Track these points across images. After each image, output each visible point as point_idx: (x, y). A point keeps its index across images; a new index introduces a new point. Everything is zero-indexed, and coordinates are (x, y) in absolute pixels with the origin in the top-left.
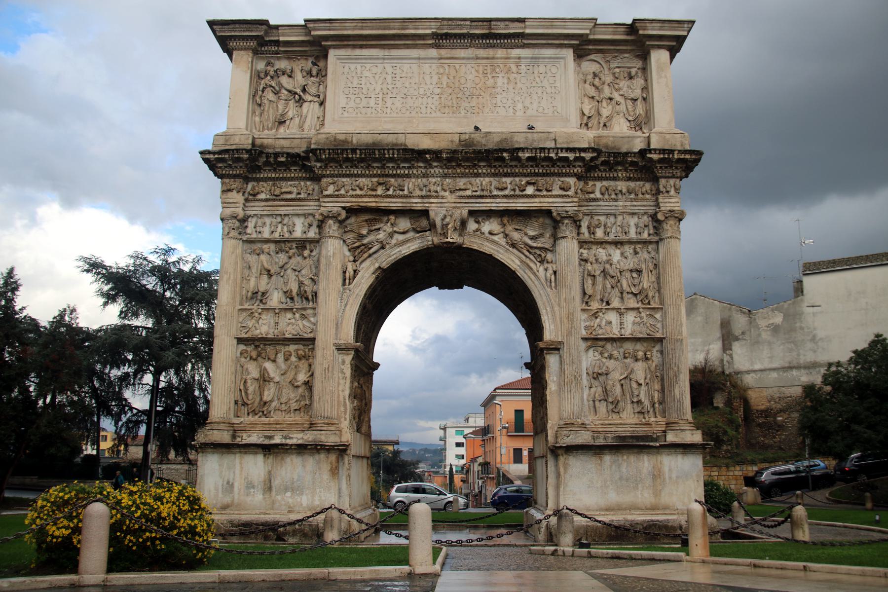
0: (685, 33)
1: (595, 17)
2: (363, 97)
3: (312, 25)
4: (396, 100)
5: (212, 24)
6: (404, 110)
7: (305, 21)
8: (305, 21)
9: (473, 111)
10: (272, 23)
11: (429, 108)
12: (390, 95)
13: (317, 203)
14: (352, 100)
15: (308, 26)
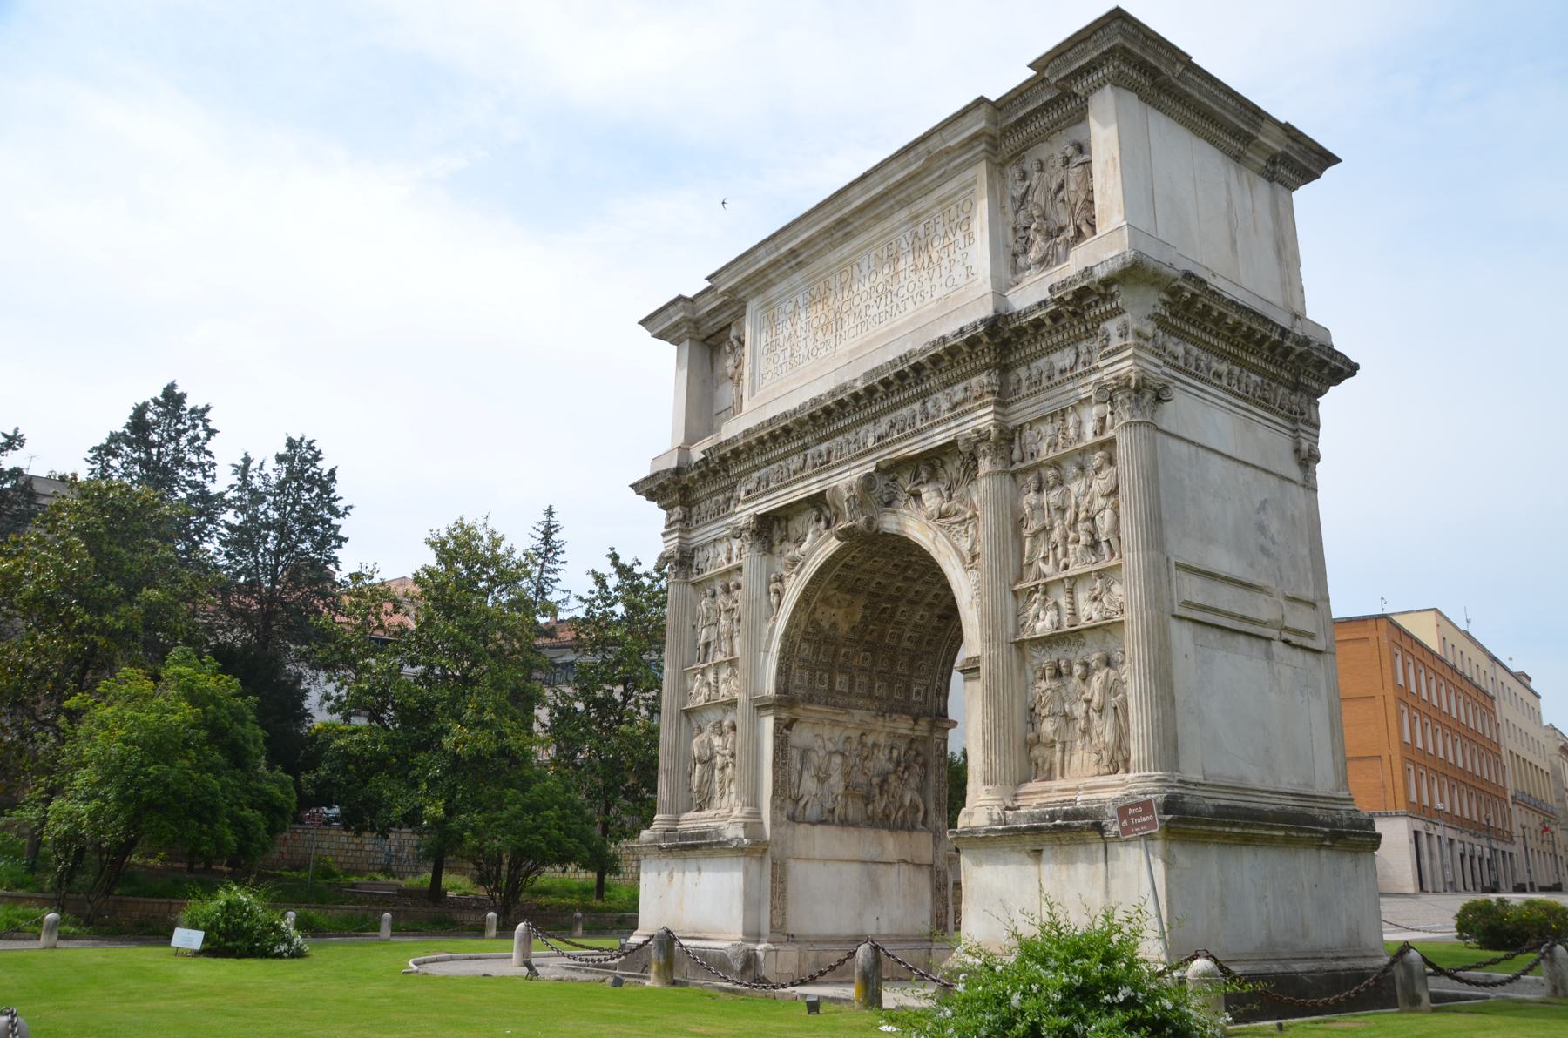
5: (643, 322)
7: (708, 279)
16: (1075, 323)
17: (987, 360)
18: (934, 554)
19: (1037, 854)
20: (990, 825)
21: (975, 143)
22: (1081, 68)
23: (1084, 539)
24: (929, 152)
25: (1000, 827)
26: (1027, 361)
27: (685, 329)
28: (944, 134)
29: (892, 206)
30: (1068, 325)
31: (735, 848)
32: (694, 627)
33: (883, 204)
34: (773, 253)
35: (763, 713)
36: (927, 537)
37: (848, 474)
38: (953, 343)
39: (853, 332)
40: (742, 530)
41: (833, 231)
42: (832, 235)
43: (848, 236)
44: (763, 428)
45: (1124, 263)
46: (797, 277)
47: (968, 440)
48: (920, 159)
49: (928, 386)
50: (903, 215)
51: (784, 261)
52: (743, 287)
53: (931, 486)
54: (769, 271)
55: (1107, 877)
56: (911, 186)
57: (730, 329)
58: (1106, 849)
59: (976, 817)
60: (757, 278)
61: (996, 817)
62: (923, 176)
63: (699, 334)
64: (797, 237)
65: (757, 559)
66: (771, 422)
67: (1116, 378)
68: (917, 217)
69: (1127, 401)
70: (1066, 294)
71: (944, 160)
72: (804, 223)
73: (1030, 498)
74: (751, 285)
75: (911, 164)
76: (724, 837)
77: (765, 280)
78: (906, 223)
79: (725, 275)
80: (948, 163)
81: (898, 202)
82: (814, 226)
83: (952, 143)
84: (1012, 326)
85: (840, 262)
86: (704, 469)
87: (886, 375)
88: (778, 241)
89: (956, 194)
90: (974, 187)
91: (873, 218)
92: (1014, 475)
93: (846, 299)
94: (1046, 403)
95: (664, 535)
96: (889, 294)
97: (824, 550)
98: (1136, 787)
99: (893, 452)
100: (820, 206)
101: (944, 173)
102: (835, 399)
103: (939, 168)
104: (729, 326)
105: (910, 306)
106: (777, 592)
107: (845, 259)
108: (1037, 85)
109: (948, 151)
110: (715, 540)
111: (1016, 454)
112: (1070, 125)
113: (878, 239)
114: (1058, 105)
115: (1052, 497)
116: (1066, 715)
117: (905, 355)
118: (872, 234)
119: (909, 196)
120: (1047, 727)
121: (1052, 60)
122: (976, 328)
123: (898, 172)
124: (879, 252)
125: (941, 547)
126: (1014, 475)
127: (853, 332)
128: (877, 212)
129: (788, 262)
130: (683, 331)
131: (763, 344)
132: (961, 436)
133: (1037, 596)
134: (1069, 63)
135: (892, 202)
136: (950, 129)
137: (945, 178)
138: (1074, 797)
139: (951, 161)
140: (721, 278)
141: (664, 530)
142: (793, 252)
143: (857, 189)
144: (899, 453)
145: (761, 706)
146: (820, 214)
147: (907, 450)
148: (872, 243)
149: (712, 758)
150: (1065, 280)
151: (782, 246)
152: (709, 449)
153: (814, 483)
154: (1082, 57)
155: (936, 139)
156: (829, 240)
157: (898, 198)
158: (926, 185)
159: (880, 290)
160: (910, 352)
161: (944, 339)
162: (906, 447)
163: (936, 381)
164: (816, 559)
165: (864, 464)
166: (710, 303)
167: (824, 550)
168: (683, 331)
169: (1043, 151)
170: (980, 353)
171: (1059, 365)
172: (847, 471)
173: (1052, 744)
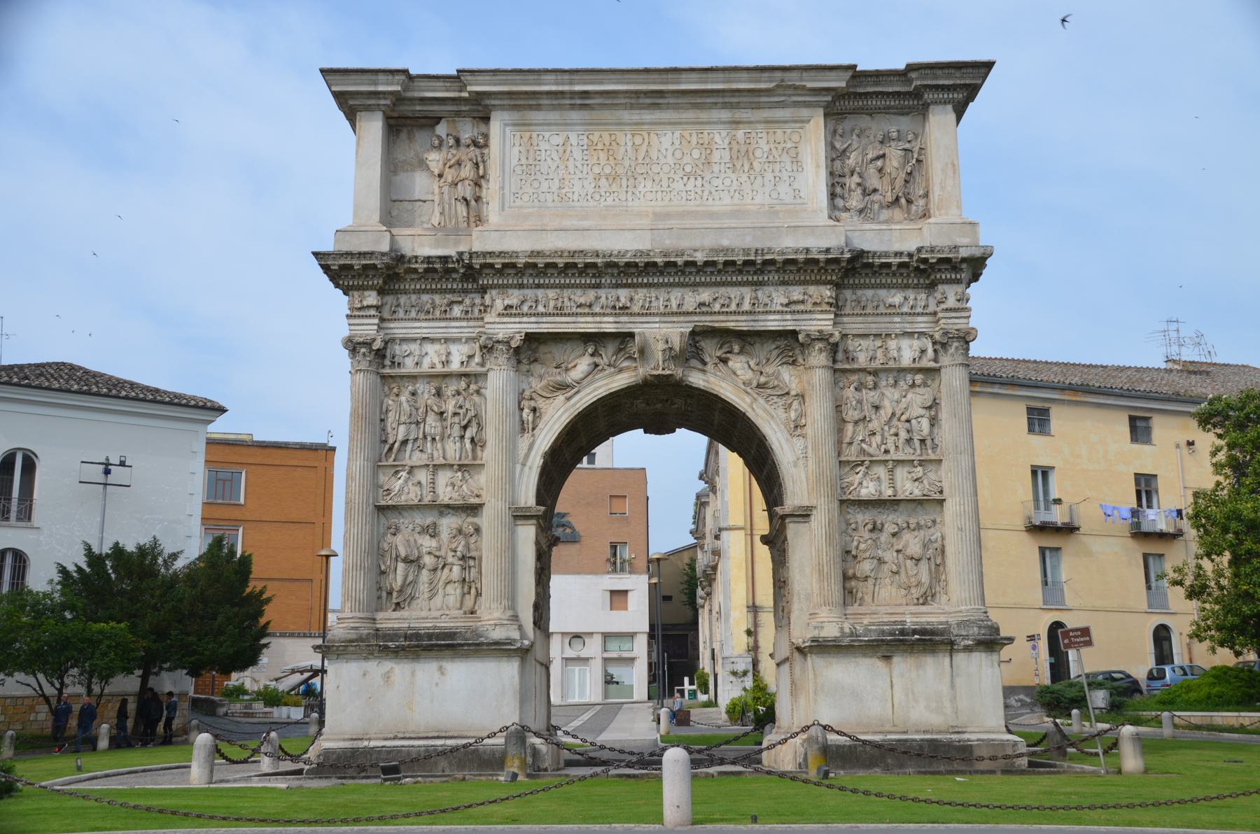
0: (979, 82)
1: (852, 62)
2: (541, 178)
3: (469, 78)
4: (586, 183)
6: (597, 196)
7: (458, 71)
8: (458, 71)
9: (689, 198)
10: (413, 72)
11: (630, 193)
13: (480, 323)
14: (528, 184)
15: (462, 78)
16: (912, 275)
17: (834, 278)
18: (750, 414)
19: (887, 658)
20: (841, 636)
21: (823, 93)
23: (903, 435)
24: (782, 81)
25: (866, 639)
26: (855, 287)
27: (388, 102)
28: (805, 74)
29: (716, 103)
30: (905, 275)
31: (518, 649)
32: (382, 420)
34: (563, 84)
35: (519, 522)
36: (743, 400)
37: (657, 325)
38: (816, 257)
39: (649, 196)
40: (498, 342)
41: (642, 95)
42: (638, 97)
45: (984, 254)
46: (575, 116)
47: (808, 335)
48: (771, 81)
49: (766, 278)
50: (725, 115)
52: (499, 96)
53: (743, 358)
54: (545, 96)
55: (952, 676)
56: (745, 96)
57: (438, 123)
58: (951, 656)
59: (825, 630)
61: (847, 630)
62: (762, 94)
63: (393, 110)
64: (601, 83)
65: (512, 373)
66: (573, 254)
67: (957, 330)
68: (738, 123)
69: (960, 348)
70: (933, 258)
71: (790, 92)
72: (618, 76)
73: (850, 392)
74: (511, 99)
75: (760, 82)
76: (487, 638)
78: (724, 123)
79: (488, 78)
80: (790, 96)
81: (726, 103)
82: (628, 83)
83: (810, 85)
84: (865, 261)
85: (636, 124)
86: (437, 266)
87: (736, 259)
88: (576, 77)
89: (786, 122)
90: (807, 126)
92: (835, 371)
93: (640, 159)
94: (873, 326)
95: (347, 316)
96: (699, 179)
97: (607, 384)
98: (972, 616)
101: (783, 101)
102: (665, 260)
103: (780, 95)
104: (438, 120)
105: (727, 200)
106: (534, 410)
107: (643, 124)
109: (796, 88)
110: (424, 338)
111: (840, 356)
112: (895, 114)
114: (893, 97)
115: (870, 396)
116: (879, 559)
117: (763, 250)
118: (684, 116)
119: (739, 103)
120: (866, 567)
122: (842, 253)
123: (744, 82)
124: (686, 134)
125: (760, 412)
126: (835, 371)
127: (649, 196)
128: (699, 101)
129: (571, 98)
130: (382, 102)
131: (515, 162)
132: (805, 330)
133: (862, 469)
134: (936, 77)
135: (720, 100)
136: (812, 73)
138: (904, 619)
139: (794, 95)
141: (349, 312)
143: (694, 76)
144: (723, 325)
145: (520, 516)
146: (641, 77)
147: (733, 324)
148: (680, 123)
149: (419, 558)
150: (935, 247)
151: (578, 84)
153: (610, 323)
154: (947, 78)
155: (795, 75)
156: (633, 101)
157: (727, 100)
158: (759, 102)
159: (688, 169)
160: (770, 249)
161: (808, 250)
162: (733, 321)
163: (776, 278)
164: (595, 390)
165: (678, 322)
167: (607, 384)
169: (864, 122)
170: (830, 271)
171: (890, 300)
172: (657, 322)
173: (866, 578)
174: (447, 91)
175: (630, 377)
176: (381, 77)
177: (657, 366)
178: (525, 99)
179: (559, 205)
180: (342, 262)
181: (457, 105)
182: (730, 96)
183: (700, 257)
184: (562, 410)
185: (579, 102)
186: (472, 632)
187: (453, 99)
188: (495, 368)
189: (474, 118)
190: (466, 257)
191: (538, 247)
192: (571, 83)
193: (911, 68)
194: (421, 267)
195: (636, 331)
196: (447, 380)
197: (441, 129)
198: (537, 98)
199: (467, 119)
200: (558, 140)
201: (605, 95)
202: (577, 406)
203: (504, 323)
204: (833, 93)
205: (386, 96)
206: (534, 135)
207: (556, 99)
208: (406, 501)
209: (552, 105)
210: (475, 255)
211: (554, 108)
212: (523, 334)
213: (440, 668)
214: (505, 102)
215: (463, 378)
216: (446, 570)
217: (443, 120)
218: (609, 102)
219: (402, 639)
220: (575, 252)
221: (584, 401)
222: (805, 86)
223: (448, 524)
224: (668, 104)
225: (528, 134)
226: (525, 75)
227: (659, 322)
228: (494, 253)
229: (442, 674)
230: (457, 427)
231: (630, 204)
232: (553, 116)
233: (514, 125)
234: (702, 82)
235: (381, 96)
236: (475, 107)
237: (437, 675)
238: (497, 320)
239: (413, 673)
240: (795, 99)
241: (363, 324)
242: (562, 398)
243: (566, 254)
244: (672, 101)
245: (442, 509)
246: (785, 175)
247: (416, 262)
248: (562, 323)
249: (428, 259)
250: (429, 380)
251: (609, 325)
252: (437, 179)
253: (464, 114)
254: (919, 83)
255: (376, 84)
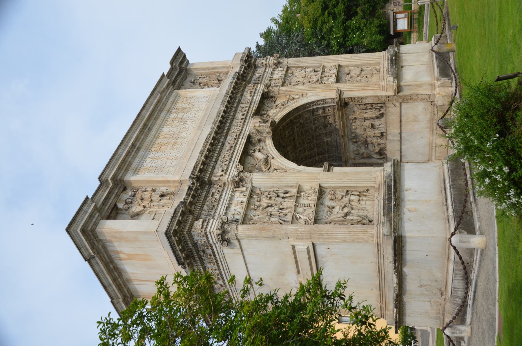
2: (164, 165)
3: (104, 176)
12: (169, 154)
21: (169, 86)
22: (182, 60)
24: (159, 92)
33: (155, 113)
34: (125, 149)
43: (150, 129)
44: (206, 146)
46: (141, 153)
48: (158, 95)
50: (164, 113)
51: (131, 151)
52: (119, 173)
54: (127, 158)
60: (123, 165)
64: (132, 138)
66: (206, 142)
71: (164, 94)
74: (122, 169)
76: (391, 173)
77: (127, 163)
78: (167, 114)
80: (165, 95)
82: (136, 130)
83: (165, 86)
85: (154, 137)
89: (175, 99)
91: (154, 119)
99: (252, 112)
100: (135, 122)
103: (164, 96)
107: (155, 135)
108: (172, 71)
109: (163, 91)
113: (162, 123)
121: (173, 61)
128: (154, 116)
129: (133, 151)
130: (97, 216)
135: (157, 111)
137: (168, 99)
139: (166, 93)
140: (107, 173)
142: (133, 145)
143: (144, 112)
146: (136, 125)
147: (254, 108)
148: (161, 125)
151: (128, 144)
152: (192, 174)
153: (241, 141)
155: (158, 88)
158: (164, 103)
161: (232, 82)
165: (248, 122)
166: (102, 196)
167: (270, 147)
168: (97, 216)
174: (105, 191)
175: (268, 140)
176: (85, 208)
177: (266, 129)
178: (124, 165)
179: (179, 160)
180: (175, 223)
181: (113, 193)
182: (158, 108)
183: (223, 108)
184: (278, 160)
185: (136, 149)
186: (387, 178)
187: (109, 193)
188: (251, 177)
189: (122, 192)
190: (192, 176)
191: (199, 151)
192: (127, 146)
193: (172, 62)
194: (190, 199)
195: (248, 133)
196: (251, 203)
197: (120, 206)
198: (127, 161)
199: (121, 195)
200: (148, 160)
201: (137, 140)
202: (277, 155)
203: (230, 173)
204: (170, 85)
205: (95, 213)
206: (143, 168)
207: (130, 156)
208: (313, 214)
209: (132, 158)
210: (193, 173)
211: (134, 158)
212: (238, 164)
213: (406, 190)
214: (122, 172)
215: (252, 196)
216: (353, 203)
217: (117, 203)
218: (141, 140)
219: (390, 205)
220: (206, 141)
221: (275, 153)
222: (164, 88)
223: (327, 202)
224: (151, 125)
225: (141, 170)
226: (115, 158)
227: (246, 127)
228: (195, 166)
229: (410, 189)
230: (277, 199)
231: (189, 139)
232: (137, 160)
233: (134, 173)
234: (148, 111)
235: (93, 215)
236: (118, 187)
237: (410, 192)
238: (227, 175)
239: (409, 201)
240: (167, 94)
241: (212, 225)
242: (272, 161)
243: (206, 144)
244: (151, 123)
245: (320, 202)
246: (196, 100)
247: (187, 200)
248: (236, 155)
249: (188, 195)
250: (249, 210)
251: (242, 141)
252: (146, 209)
253: (119, 193)
254: (178, 64)
255: (87, 212)
